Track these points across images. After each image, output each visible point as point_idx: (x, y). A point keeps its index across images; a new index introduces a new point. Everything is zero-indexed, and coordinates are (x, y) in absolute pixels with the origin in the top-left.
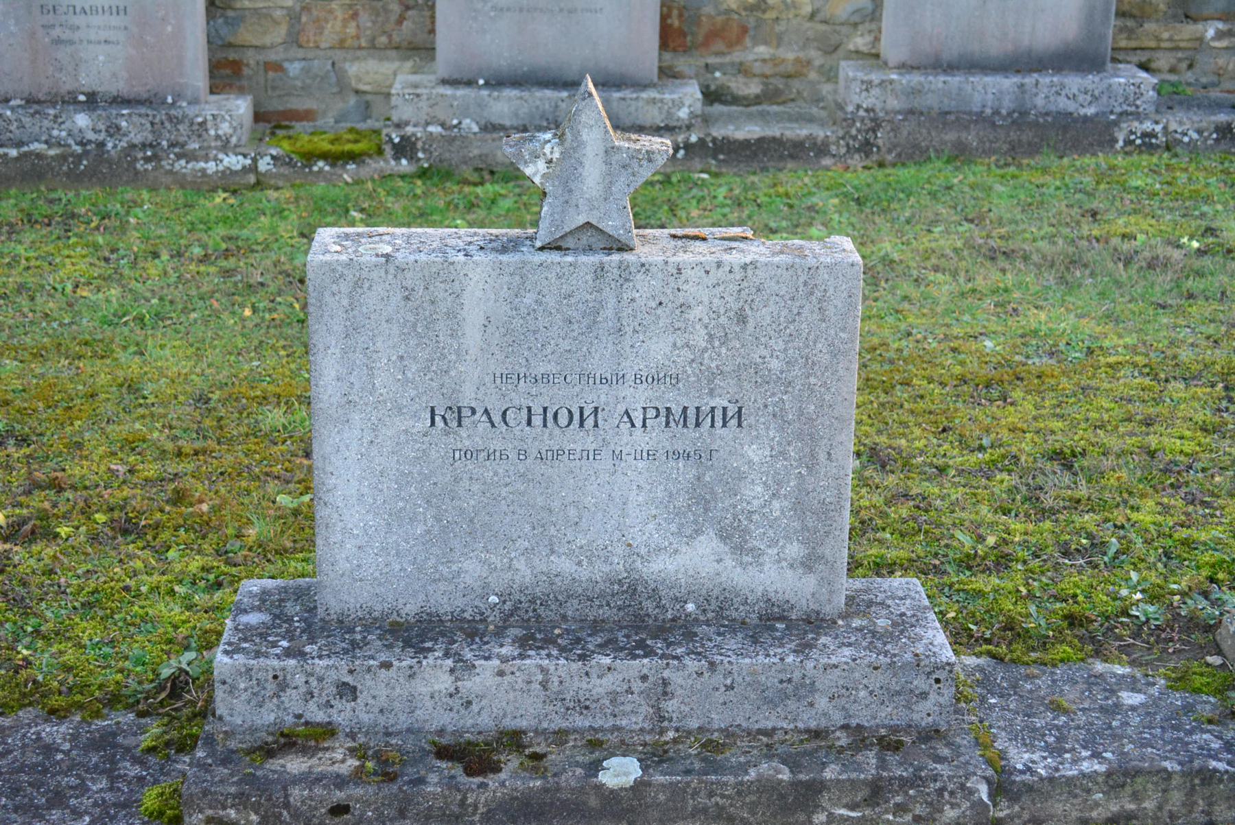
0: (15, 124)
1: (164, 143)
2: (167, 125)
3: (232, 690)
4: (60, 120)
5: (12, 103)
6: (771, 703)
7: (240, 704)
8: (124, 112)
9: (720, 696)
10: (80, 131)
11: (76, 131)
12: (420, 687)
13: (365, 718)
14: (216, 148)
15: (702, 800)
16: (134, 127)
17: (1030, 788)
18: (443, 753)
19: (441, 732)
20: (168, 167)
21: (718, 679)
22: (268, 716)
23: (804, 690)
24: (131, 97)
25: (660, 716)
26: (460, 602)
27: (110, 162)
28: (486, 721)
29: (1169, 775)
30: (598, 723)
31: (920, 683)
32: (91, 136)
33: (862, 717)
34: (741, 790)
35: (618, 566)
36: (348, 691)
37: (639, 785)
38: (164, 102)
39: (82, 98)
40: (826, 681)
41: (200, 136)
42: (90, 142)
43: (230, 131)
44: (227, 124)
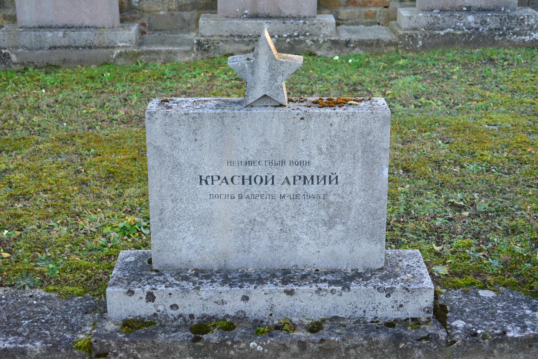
0: (442, 20)
1: (505, 28)
2: (507, 20)
4: (461, 18)
5: (434, 11)
8: (489, 14)
10: (469, 23)
11: (467, 23)
14: (527, 30)
16: (492, 21)
20: (508, 39)
24: (486, 8)
27: (484, 37)
32: (473, 25)
38: (500, 10)
39: (465, 9)
41: (520, 25)
42: (472, 28)
43: (534, 22)
44: (533, 19)
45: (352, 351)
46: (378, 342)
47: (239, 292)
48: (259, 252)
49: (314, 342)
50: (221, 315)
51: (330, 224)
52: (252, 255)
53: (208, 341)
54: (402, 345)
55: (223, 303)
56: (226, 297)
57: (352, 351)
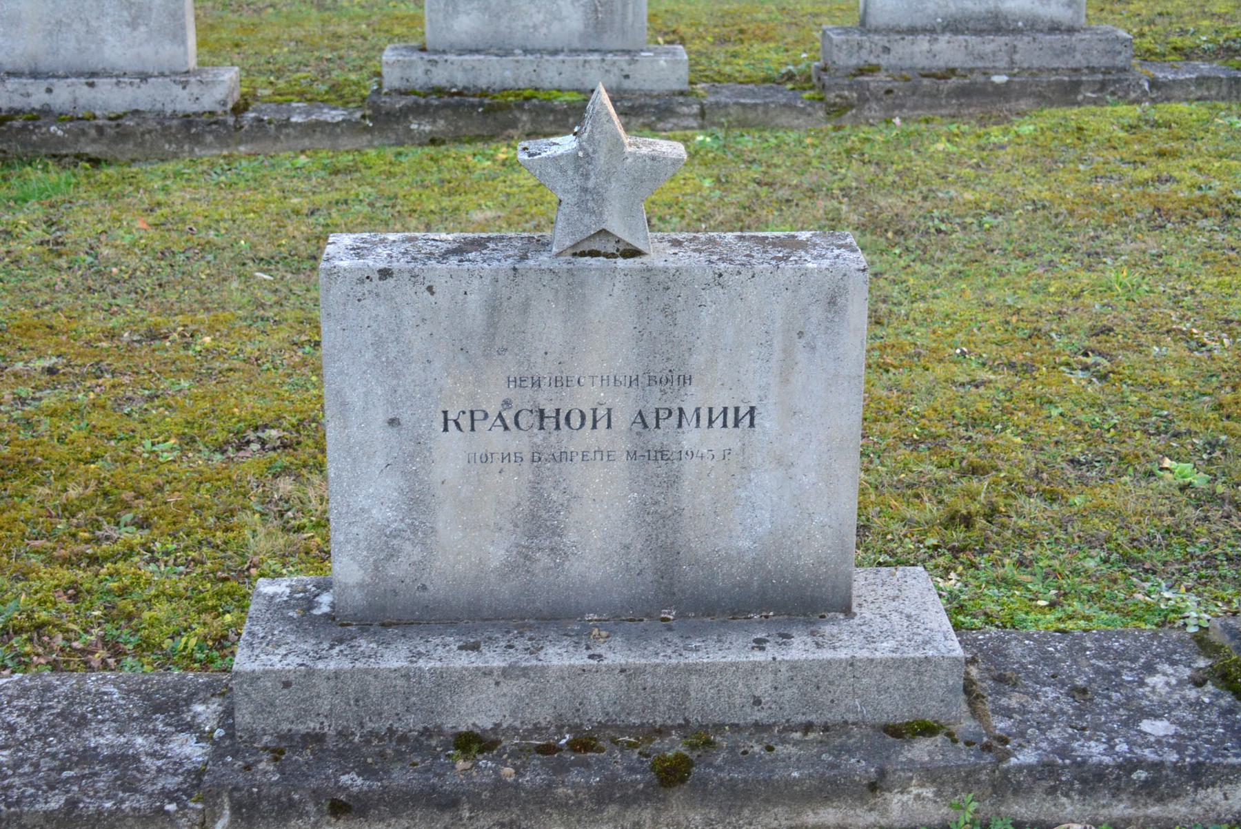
3: (840, 50)
6: (1058, 56)
7: (843, 56)
9: (1037, 53)
12: (916, 49)
15: (1034, 88)
19: (923, 69)
21: (1036, 45)
22: (854, 61)
23: (1070, 50)
26: (925, 21)
28: (941, 64)
29: (1221, 80)
30: (988, 65)
31: (1118, 47)
33: (1094, 63)
34: (1049, 84)
36: (886, 50)
37: (1008, 83)
40: (1080, 47)
45: (147, 136)
46: (170, 127)
47: (44, 84)
48: (68, 51)
49: (110, 127)
50: (27, 109)
51: (133, 24)
52: (61, 58)
53: (11, 127)
54: (193, 130)
55: (28, 95)
56: (31, 89)
57: (147, 136)
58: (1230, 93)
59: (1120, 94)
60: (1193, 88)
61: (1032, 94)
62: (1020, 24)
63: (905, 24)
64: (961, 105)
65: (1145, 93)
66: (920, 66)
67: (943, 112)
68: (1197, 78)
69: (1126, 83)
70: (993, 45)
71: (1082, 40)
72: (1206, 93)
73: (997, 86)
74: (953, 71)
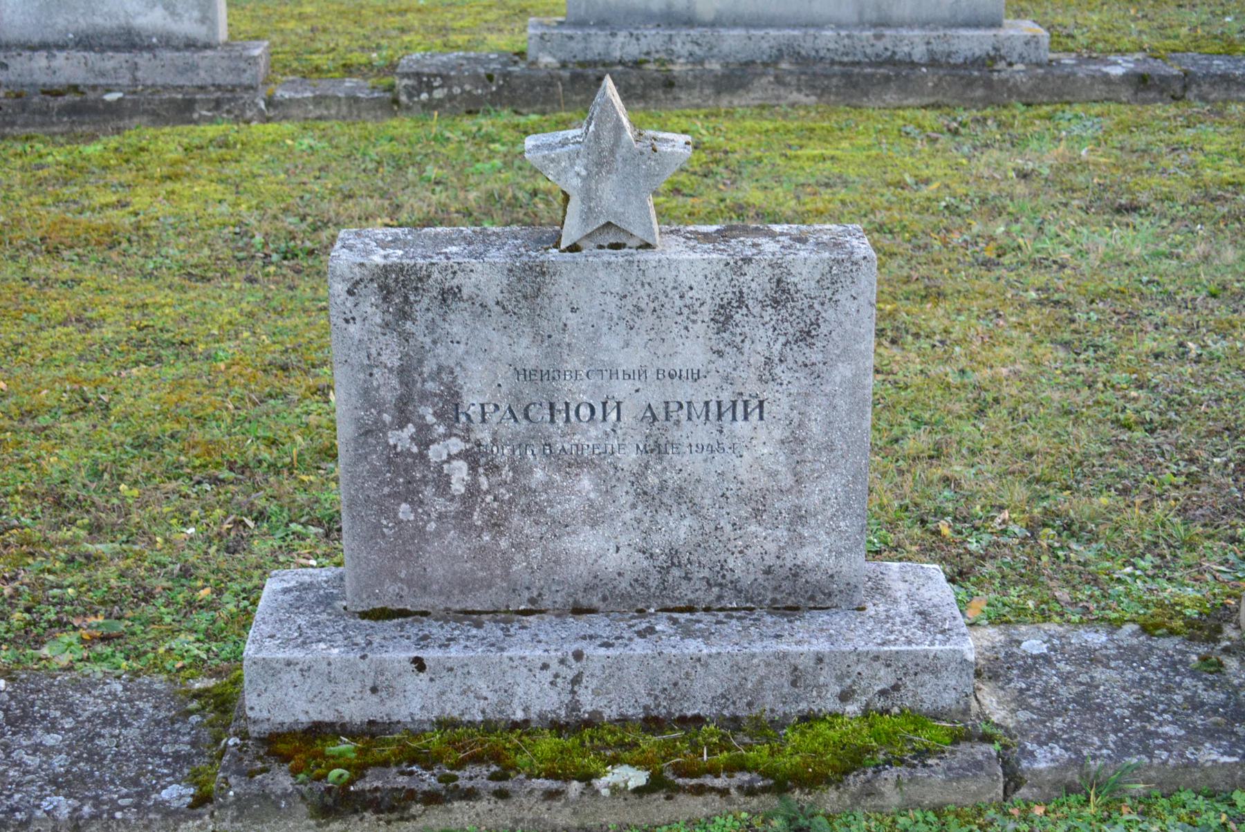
6: (182, 74)
9: (159, 70)
12: (34, 65)
13: (13, 78)
15: (146, 106)
17: (281, 103)
18: (44, 93)
19: (44, 85)
21: (158, 62)
23: (193, 68)
25: (135, 79)
26: (57, 37)
28: (62, 80)
29: (339, 99)
30: (110, 82)
31: (242, 65)
33: (220, 80)
34: (162, 102)
35: (123, 21)
37: (119, 100)
40: (203, 64)
58: (350, 112)
59: (237, 112)
60: (311, 107)
61: (145, 112)
62: (154, 40)
63: (36, 40)
64: (73, 122)
65: (261, 110)
66: (41, 82)
67: (56, 129)
68: (315, 98)
69: (241, 102)
70: (113, 61)
71: (203, 58)
72: (325, 113)
73: (109, 104)
74: (75, 88)
